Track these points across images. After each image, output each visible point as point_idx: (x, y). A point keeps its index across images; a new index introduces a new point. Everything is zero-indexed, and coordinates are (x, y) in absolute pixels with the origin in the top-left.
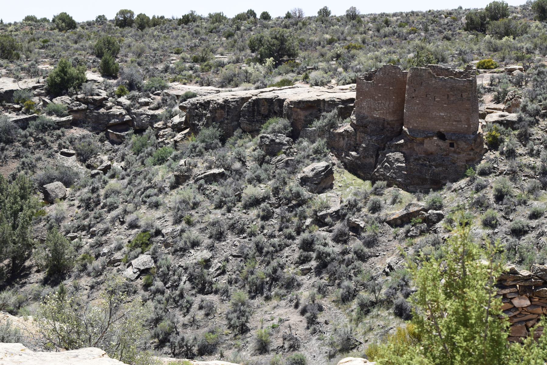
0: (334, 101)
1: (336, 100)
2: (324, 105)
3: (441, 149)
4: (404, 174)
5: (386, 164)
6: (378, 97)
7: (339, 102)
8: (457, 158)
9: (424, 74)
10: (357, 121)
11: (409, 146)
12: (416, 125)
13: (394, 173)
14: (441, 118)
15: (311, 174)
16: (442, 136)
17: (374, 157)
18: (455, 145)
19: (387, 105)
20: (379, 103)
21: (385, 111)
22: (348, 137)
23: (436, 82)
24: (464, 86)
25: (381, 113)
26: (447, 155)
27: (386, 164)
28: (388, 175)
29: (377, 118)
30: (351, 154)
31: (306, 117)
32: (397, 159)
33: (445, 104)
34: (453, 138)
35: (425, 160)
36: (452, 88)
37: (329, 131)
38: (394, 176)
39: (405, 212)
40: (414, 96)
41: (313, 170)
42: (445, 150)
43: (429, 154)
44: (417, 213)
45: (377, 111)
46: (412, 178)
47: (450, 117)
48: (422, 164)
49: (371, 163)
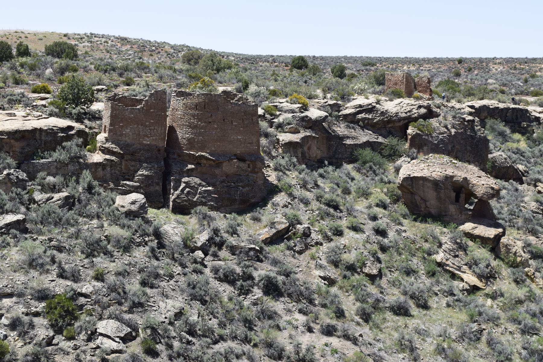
0: (52, 129)
1: (54, 128)
2: (41, 134)
3: (243, 171)
4: (214, 197)
5: (187, 189)
6: (150, 122)
7: (57, 130)
8: (257, 178)
9: (219, 100)
10: (121, 149)
11: (199, 170)
12: (213, 149)
13: (201, 197)
14: (237, 141)
15: (134, 208)
16: (241, 159)
17: (161, 184)
18: (251, 165)
19: (159, 131)
20: (150, 129)
21: (157, 138)
22: (111, 167)
23: (232, 107)
24: (253, 110)
25: (153, 139)
26: (248, 175)
27: (187, 189)
28: (195, 199)
29: (148, 145)
30: (126, 184)
31: (23, 148)
32: (200, 183)
33: (241, 127)
34: (253, 159)
35: (228, 182)
36: (245, 112)
37: (78, 162)
38: (203, 200)
39: (274, 231)
40: (210, 121)
41: (133, 203)
42: (246, 171)
43: (227, 176)
44: (287, 230)
45: (148, 137)
46: (222, 201)
47: (245, 140)
48: (227, 186)
49: (157, 191)
